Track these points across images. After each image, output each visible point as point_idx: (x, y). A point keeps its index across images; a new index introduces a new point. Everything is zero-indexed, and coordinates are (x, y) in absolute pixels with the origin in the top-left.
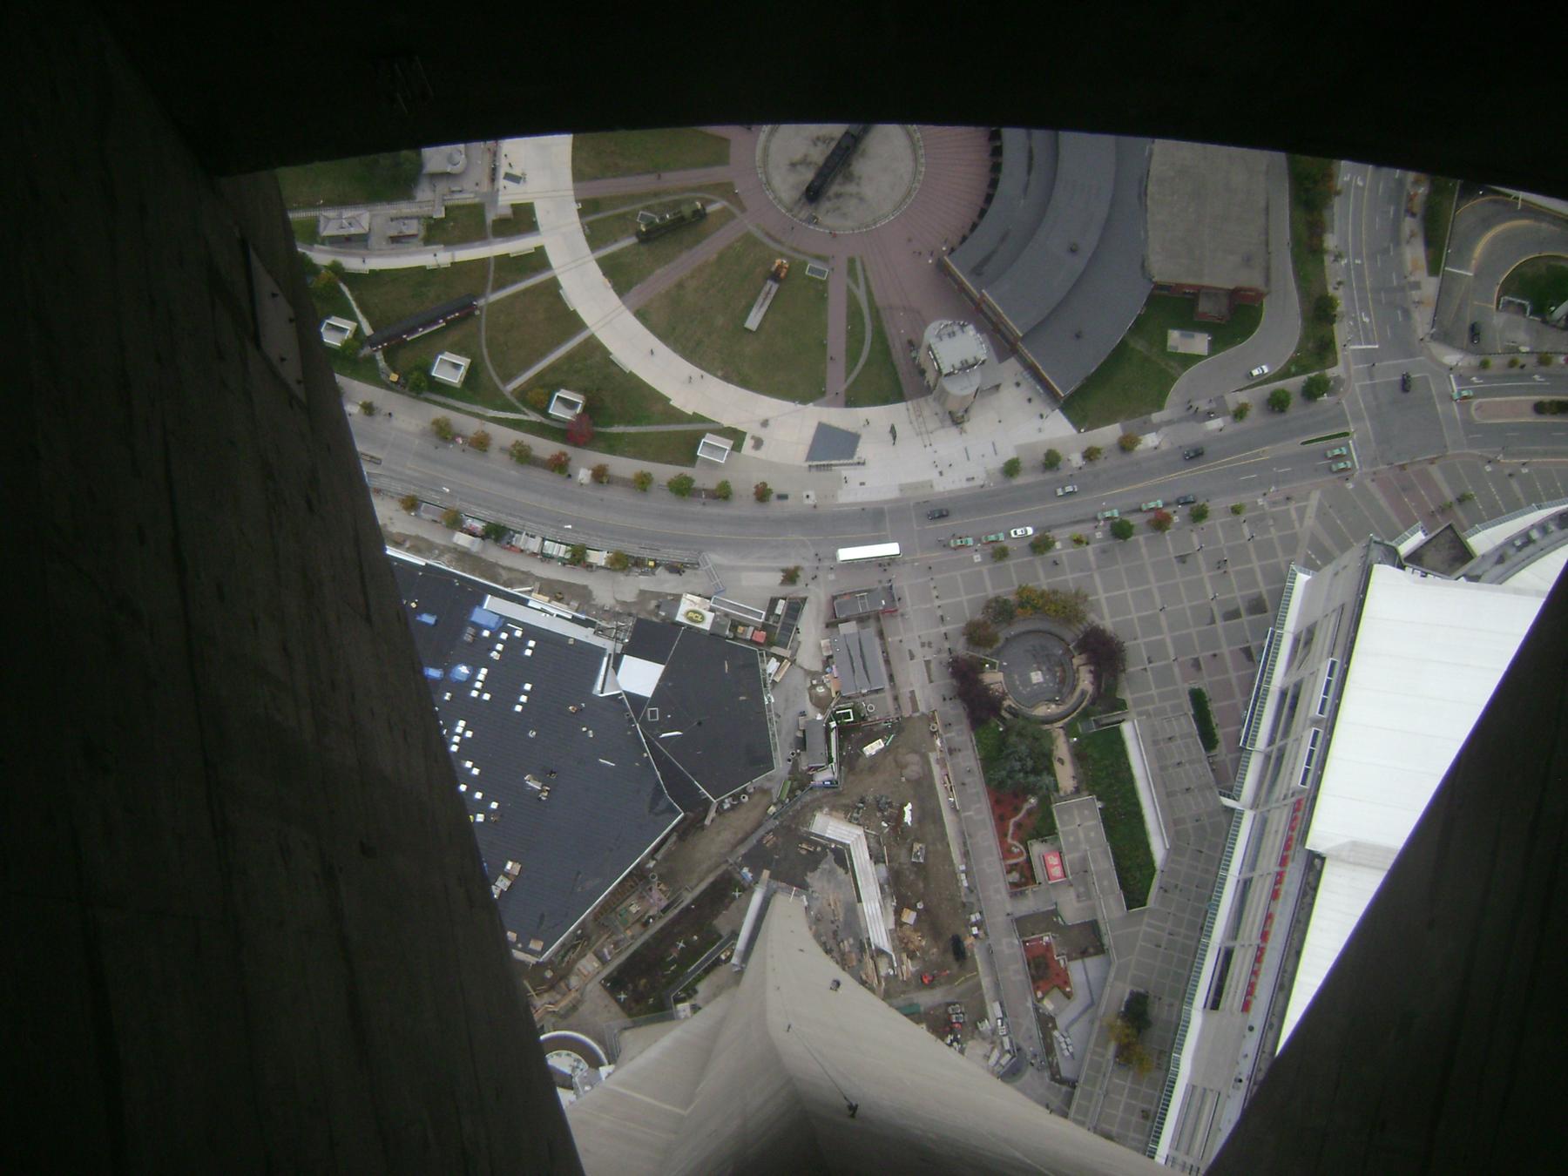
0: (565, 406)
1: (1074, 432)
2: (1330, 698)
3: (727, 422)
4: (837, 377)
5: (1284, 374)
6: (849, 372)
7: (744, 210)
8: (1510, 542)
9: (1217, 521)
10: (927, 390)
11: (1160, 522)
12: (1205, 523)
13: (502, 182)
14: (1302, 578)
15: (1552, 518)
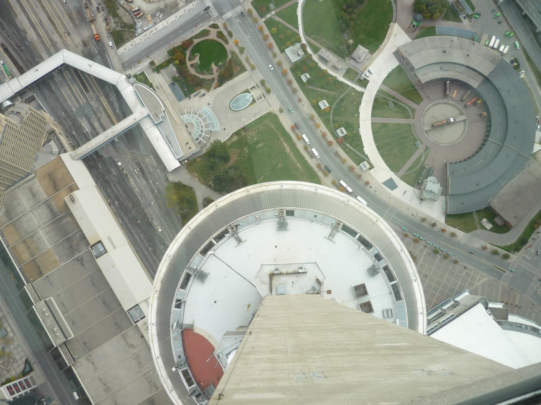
0: (342, 132)
1: (444, 222)
2: (446, 321)
3: (372, 162)
4: (402, 172)
5: (503, 248)
6: (406, 172)
7: (413, 118)
8: (517, 323)
9: (458, 267)
10: (420, 189)
11: (446, 257)
12: (456, 265)
13: (366, 72)
14: (466, 294)
15: (531, 327)
